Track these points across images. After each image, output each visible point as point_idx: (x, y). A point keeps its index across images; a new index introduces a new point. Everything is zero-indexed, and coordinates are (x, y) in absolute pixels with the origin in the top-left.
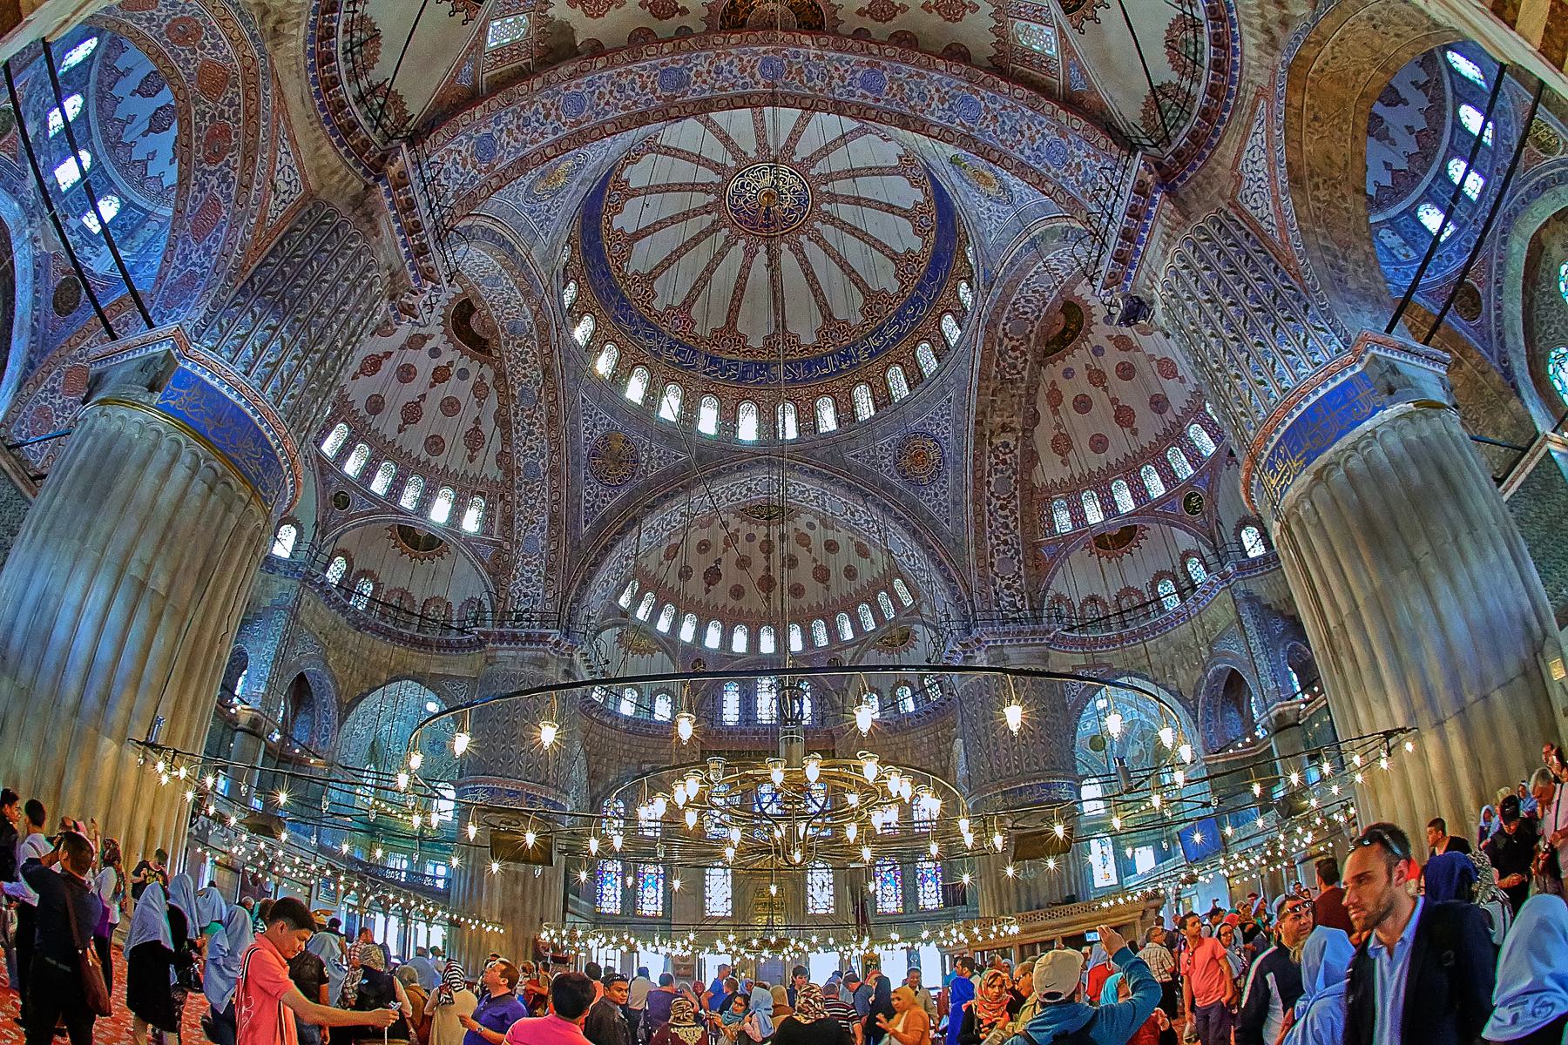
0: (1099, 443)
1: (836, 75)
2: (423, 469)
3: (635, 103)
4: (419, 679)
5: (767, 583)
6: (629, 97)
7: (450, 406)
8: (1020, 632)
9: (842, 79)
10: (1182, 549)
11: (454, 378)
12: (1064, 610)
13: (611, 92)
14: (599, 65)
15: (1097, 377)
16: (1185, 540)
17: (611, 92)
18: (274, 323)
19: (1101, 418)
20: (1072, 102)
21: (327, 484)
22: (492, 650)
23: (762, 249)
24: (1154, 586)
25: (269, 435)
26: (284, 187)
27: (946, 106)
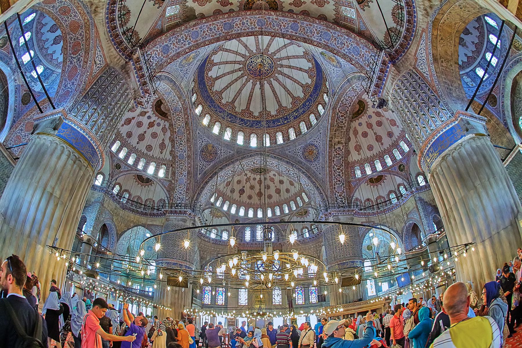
0: (370, 148)
1: (282, 25)
2: (145, 156)
3: (216, 34)
4: (144, 226)
5: (260, 194)
6: (213, 32)
7: (154, 135)
8: (344, 211)
9: (285, 26)
10: (398, 182)
11: (156, 126)
12: (359, 203)
13: (207, 31)
14: (203, 22)
15: (370, 126)
16: (399, 180)
17: (207, 31)
18: (95, 107)
19: (371, 139)
20: (361, 34)
21: (113, 161)
22: (168, 216)
23: (258, 83)
24: (388, 195)
25: (94, 145)
26: (99, 62)
27: (319, 35)
